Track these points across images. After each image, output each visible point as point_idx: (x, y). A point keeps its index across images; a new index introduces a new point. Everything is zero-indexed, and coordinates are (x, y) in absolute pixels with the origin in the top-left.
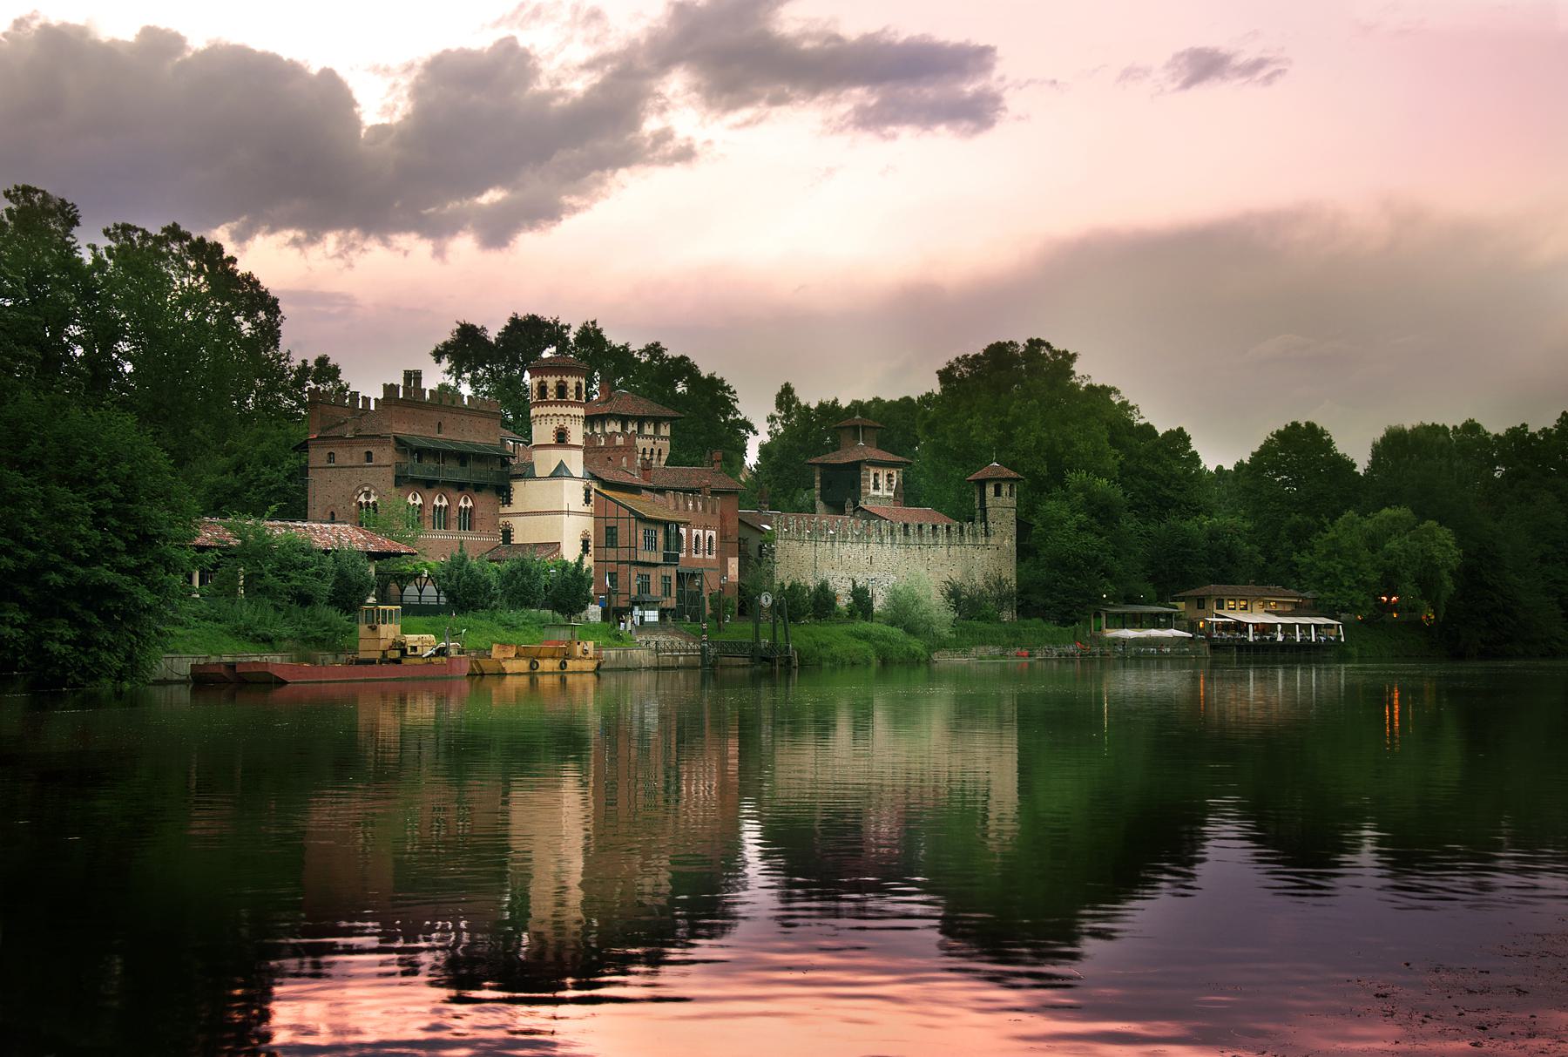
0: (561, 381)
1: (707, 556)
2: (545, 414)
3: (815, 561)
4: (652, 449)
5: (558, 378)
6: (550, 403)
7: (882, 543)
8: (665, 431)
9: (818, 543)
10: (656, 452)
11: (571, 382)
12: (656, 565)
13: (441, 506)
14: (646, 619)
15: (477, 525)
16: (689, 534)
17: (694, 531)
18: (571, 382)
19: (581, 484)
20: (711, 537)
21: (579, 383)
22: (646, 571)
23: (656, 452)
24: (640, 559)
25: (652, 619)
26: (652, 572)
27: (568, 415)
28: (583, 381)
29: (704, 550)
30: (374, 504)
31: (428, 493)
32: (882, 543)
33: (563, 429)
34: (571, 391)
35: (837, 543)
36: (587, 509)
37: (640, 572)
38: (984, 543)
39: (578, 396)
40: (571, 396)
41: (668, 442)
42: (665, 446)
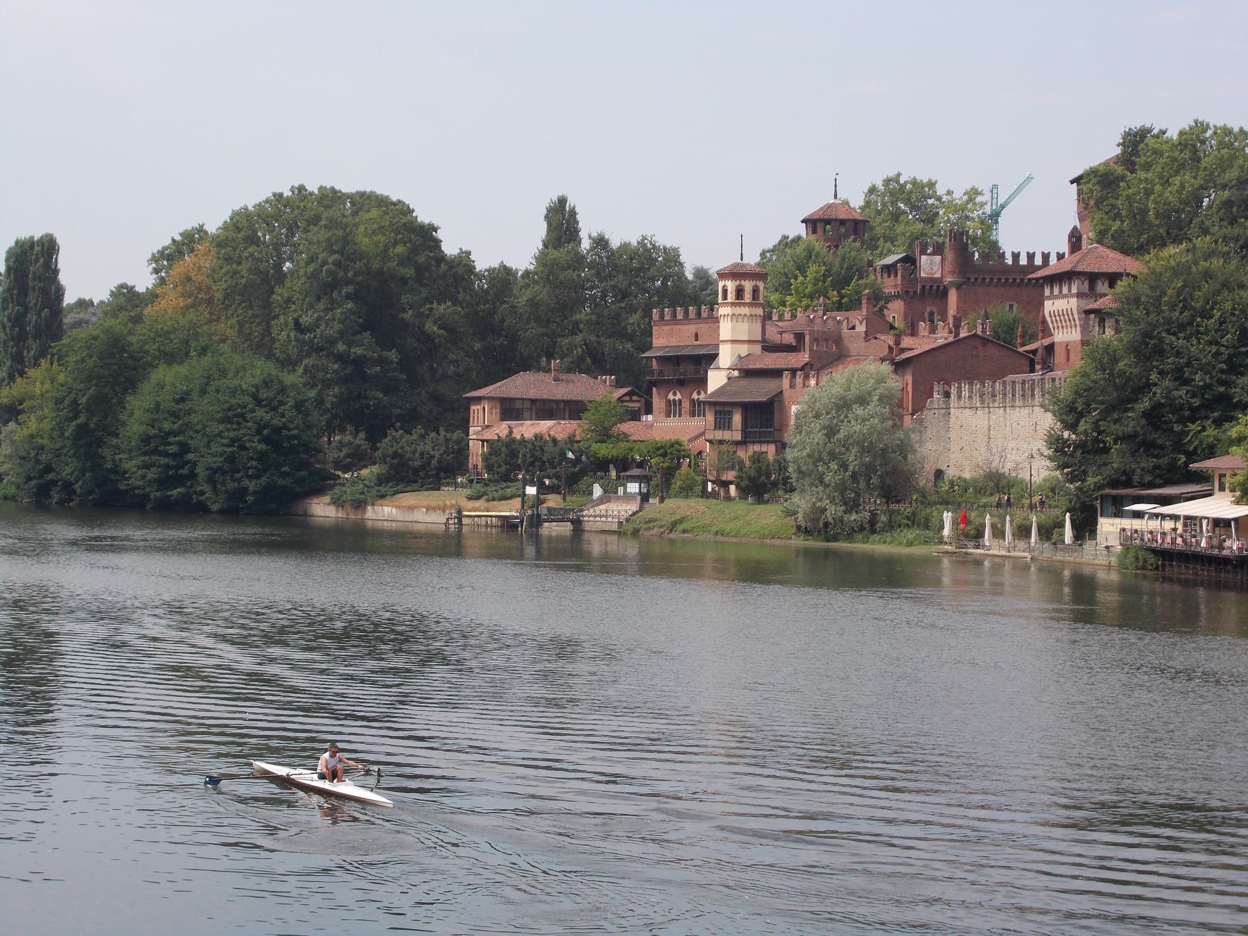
0: (740, 285)
3: (989, 430)
6: (745, 304)
9: (991, 410)
13: (674, 400)
14: (628, 490)
27: (740, 315)
30: (680, 401)
40: (748, 298)
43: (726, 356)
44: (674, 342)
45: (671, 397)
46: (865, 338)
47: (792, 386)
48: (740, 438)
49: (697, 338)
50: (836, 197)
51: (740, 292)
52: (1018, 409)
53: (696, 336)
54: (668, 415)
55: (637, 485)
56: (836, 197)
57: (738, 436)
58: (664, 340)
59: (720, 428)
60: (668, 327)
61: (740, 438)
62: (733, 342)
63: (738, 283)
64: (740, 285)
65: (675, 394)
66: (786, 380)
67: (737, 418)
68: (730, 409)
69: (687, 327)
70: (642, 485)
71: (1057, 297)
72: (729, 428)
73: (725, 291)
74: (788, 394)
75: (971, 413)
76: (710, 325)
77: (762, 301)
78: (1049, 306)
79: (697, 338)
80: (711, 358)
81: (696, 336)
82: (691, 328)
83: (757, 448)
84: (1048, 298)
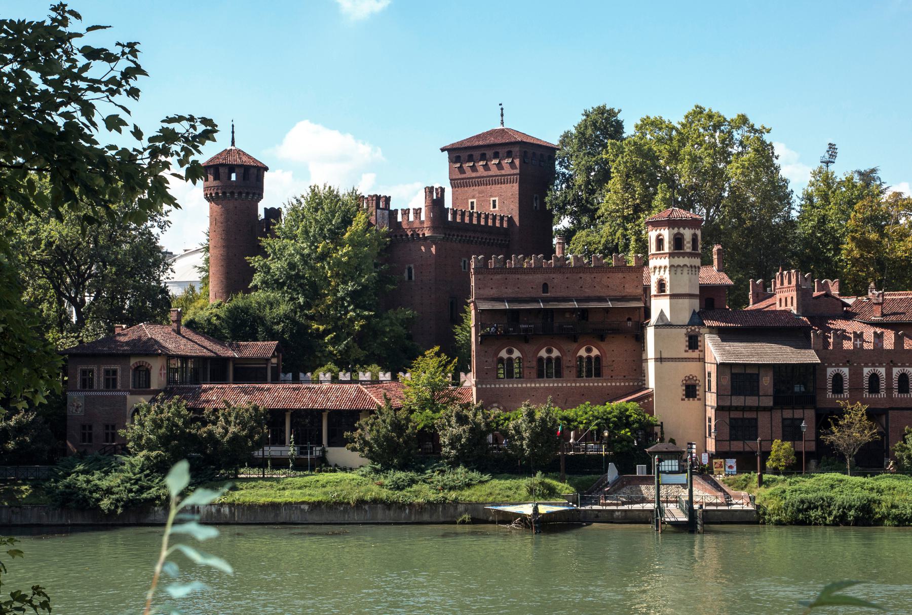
0: (678, 233)
1: (896, 394)
2: (658, 266)
5: (658, 232)
11: (687, 233)
12: (765, 409)
15: (605, 371)
16: (856, 374)
17: (866, 371)
18: (687, 233)
19: (684, 331)
20: (903, 378)
21: (695, 236)
22: (747, 415)
24: (721, 404)
28: (699, 232)
29: (889, 389)
31: (526, 347)
33: (663, 280)
34: (688, 242)
36: (695, 354)
37: (732, 416)
39: (695, 246)
44: (509, 292)
45: (504, 354)
48: (771, 404)
50: (233, 144)
56: (233, 144)
57: (769, 402)
58: (494, 291)
60: (499, 277)
63: (692, 231)
67: (767, 382)
68: (755, 371)
69: (531, 277)
73: (660, 242)
76: (569, 275)
77: (700, 252)
82: (539, 278)
83: (788, 414)
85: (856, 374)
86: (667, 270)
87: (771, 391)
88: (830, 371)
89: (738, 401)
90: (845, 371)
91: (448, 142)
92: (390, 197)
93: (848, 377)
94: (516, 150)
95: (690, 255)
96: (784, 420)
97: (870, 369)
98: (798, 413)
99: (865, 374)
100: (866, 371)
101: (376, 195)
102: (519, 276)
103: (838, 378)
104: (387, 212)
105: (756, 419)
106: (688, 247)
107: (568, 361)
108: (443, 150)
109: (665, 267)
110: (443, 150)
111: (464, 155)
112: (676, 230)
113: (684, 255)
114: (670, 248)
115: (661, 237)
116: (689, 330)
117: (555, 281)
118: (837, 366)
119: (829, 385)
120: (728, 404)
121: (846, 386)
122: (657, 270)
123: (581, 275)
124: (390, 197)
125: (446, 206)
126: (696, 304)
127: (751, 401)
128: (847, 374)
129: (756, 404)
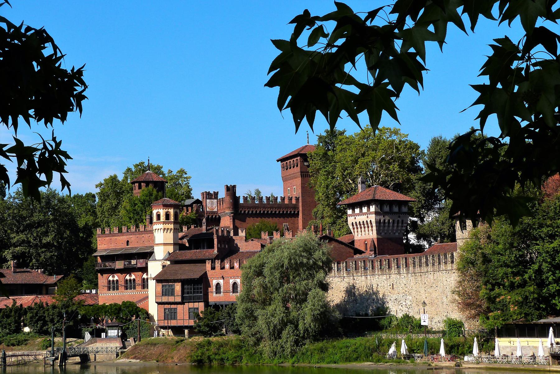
4: (367, 221)
7: (399, 273)
8: (373, 208)
10: (369, 223)
14: (109, 335)
16: (226, 283)
22: (173, 306)
23: (369, 223)
25: (113, 335)
26: (180, 307)
28: (171, 211)
32: (399, 273)
35: (369, 277)
38: (450, 268)
41: (374, 215)
42: (373, 218)
43: (160, 253)
44: (112, 246)
46: (246, 240)
47: (213, 268)
48: (180, 300)
49: (127, 245)
51: (167, 216)
52: (377, 276)
53: (128, 242)
54: (109, 289)
55: (116, 331)
57: (179, 299)
59: (166, 295)
60: (108, 238)
61: (180, 300)
62: (165, 244)
64: (168, 212)
65: (113, 277)
66: (208, 265)
67: (178, 287)
69: (121, 237)
70: (119, 331)
71: (358, 215)
72: (172, 293)
74: (210, 273)
75: (340, 280)
78: (351, 220)
79: (127, 245)
80: (148, 255)
81: (128, 242)
82: (124, 238)
83: (191, 305)
84: (351, 215)
85: (226, 283)
86: (172, 231)
87: (180, 293)
88: (214, 282)
89: (165, 299)
90: (221, 282)
91: (280, 156)
92: (218, 192)
93: (223, 285)
94: (299, 158)
95: (164, 223)
96: (189, 309)
97: (233, 280)
98: (196, 305)
99: (230, 283)
100: (231, 281)
101: (206, 192)
102: (116, 237)
103: (218, 285)
104: (216, 200)
105: (176, 308)
106: (163, 218)
107: (138, 281)
108: (278, 161)
109: (171, 229)
110: (278, 161)
111: (285, 163)
112: (157, 210)
113: (160, 223)
114: (163, 219)
115: (168, 213)
116: (163, 262)
117: (132, 239)
118: (217, 278)
119: (214, 290)
120: (160, 301)
121: (222, 290)
122: (169, 230)
123: (143, 235)
124: (218, 192)
125: (237, 195)
126: (171, 249)
127: (171, 299)
128: (222, 283)
129: (173, 301)
